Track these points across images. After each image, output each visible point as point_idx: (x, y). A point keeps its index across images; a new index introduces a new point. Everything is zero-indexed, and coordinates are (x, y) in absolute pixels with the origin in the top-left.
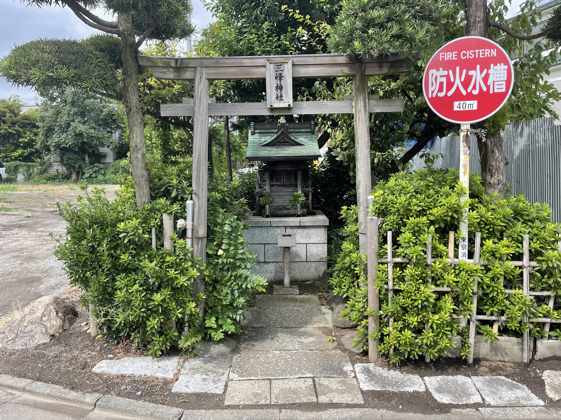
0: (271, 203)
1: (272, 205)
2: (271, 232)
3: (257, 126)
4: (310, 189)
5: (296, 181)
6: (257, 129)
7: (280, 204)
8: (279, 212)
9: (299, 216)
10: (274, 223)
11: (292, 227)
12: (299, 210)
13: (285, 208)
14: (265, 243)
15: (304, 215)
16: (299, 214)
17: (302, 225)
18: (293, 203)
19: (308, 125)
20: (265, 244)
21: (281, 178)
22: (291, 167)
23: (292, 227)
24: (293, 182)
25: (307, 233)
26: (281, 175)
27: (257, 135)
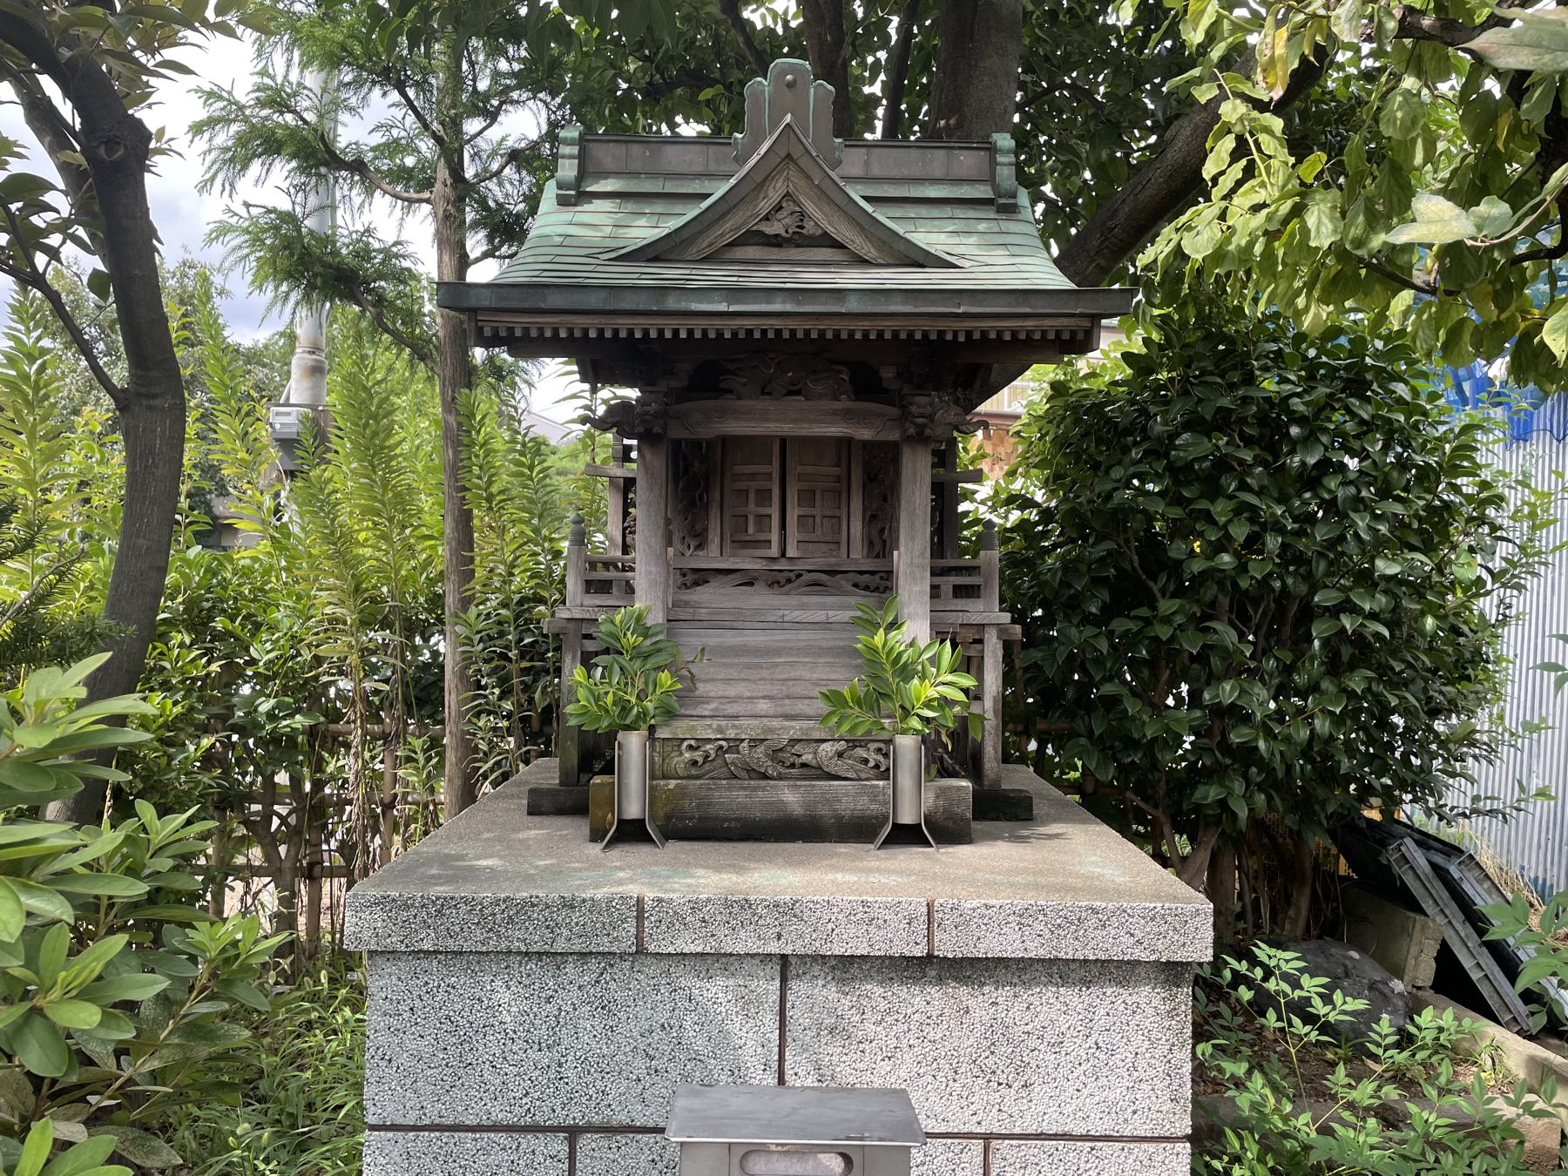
0: (669, 714)
1: (680, 728)
2: (644, 1002)
3: (606, 154)
4: (989, 611)
5: (882, 542)
6: (606, 175)
7: (749, 728)
8: (736, 798)
9: (906, 836)
10: (676, 920)
11: (847, 968)
12: (906, 780)
13: (788, 762)
14: (575, 1116)
15: (942, 830)
16: (907, 817)
17: (946, 947)
18: (863, 722)
19: (967, 161)
20: (573, 1133)
21: (762, 520)
22: (847, 416)
23: (847, 968)
24: (858, 557)
25: (996, 1034)
26: (764, 496)
27: (598, 205)
